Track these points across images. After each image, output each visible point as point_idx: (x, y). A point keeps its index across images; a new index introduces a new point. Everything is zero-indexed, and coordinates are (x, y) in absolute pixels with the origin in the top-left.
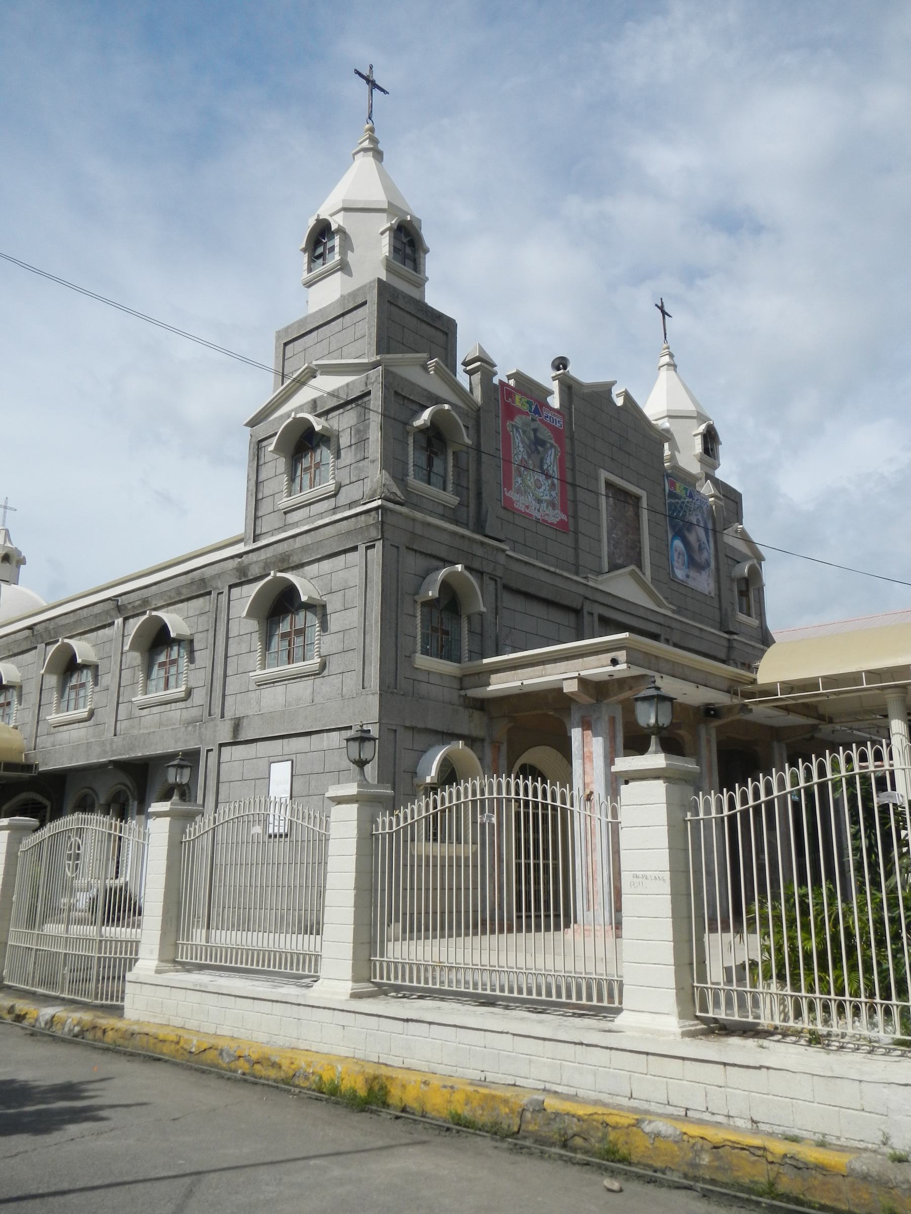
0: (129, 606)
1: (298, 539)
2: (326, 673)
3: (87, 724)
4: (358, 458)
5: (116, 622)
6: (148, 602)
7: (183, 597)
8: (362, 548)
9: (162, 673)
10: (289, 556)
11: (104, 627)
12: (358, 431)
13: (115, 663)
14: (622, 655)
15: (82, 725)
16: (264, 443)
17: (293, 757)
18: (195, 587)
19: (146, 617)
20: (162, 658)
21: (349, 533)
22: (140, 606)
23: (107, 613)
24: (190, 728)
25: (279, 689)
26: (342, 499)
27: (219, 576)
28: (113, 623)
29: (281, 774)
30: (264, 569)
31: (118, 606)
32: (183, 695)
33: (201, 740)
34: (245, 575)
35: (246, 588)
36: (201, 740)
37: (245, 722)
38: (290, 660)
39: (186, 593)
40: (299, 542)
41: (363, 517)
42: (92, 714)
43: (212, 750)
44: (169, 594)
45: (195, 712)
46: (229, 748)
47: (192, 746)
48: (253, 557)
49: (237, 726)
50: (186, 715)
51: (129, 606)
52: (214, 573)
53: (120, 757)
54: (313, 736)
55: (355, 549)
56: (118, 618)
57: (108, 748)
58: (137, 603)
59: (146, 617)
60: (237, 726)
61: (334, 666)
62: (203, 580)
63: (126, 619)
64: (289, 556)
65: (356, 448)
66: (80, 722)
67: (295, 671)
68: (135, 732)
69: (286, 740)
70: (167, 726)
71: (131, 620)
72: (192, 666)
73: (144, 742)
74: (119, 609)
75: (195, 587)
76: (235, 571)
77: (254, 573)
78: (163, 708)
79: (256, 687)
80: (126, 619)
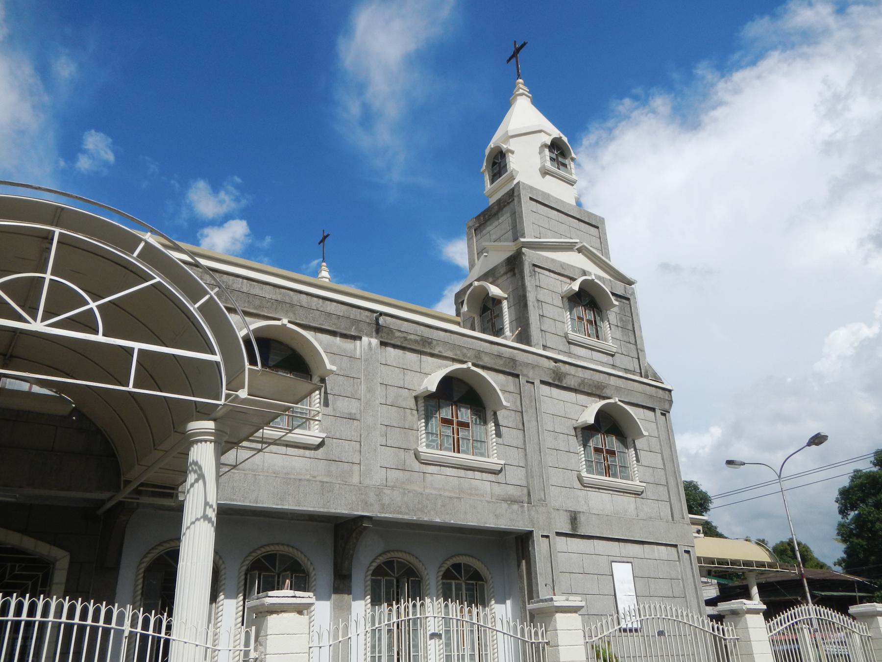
0: (398, 334)
1: (612, 378)
2: (644, 495)
3: (308, 453)
4: (625, 338)
5: (365, 339)
6: (430, 343)
7: (481, 363)
8: (658, 412)
9: (449, 432)
10: (604, 387)
11: (333, 333)
12: (621, 320)
13: (370, 390)
14: (700, 528)
15: (291, 451)
16: (537, 269)
17: (632, 560)
18: (501, 362)
19: (464, 366)
20: (446, 412)
21: (651, 396)
22: (416, 341)
23: (356, 322)
24: (515, 507)
25: (605, 496)
26: (619, 360)
27: (534, 367)
28: (360, 338)
29: (623, 573)
30: (580, 385)
31: (377, 323)
32: (498, 468)
33: (533, 525)
34: (560, 380)
35: (555, 392)
36: (533, 525)
37: (582, 518)
38: (608, 471)
39: (487, 361)
40: (613, 381)
41: (660, 391)
42: (322, 444)
43: (547, 537)
44: (465, 351)
45: (512, 491)
46: (563, 538)
47: (521, 525)
48: (572, 370)
49: (574, 519)
50: (498, 490)
51: (398, 334)
52: (526, 361)
53: (400, 516)
54: (646, 546)
55: (653, 410)
56: (370, 335)
57: (372, 498)
58: (412, 337)
59: (464, 366)
60: (574, 519)
61: (649, 494)
62: (513, 361)
63: (383, 344)
64: (604, 387)
65: (622, 332)
66: (287, 446)
67: (623, 486)
68: (420, 490)
69: (622, 544)
70: (471, 494)
71: (390, 350)
72: (500, 440)
73: (443, 506)
74: (378, 329)
75: (501, 362)
76: (551, 372)
77: (569, 383)
78: (462, 473)
79: (580, 486)
80: (383, 344)
